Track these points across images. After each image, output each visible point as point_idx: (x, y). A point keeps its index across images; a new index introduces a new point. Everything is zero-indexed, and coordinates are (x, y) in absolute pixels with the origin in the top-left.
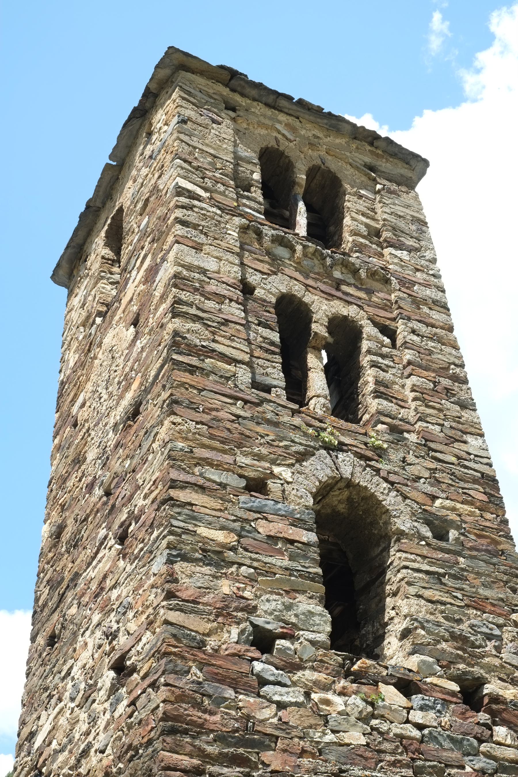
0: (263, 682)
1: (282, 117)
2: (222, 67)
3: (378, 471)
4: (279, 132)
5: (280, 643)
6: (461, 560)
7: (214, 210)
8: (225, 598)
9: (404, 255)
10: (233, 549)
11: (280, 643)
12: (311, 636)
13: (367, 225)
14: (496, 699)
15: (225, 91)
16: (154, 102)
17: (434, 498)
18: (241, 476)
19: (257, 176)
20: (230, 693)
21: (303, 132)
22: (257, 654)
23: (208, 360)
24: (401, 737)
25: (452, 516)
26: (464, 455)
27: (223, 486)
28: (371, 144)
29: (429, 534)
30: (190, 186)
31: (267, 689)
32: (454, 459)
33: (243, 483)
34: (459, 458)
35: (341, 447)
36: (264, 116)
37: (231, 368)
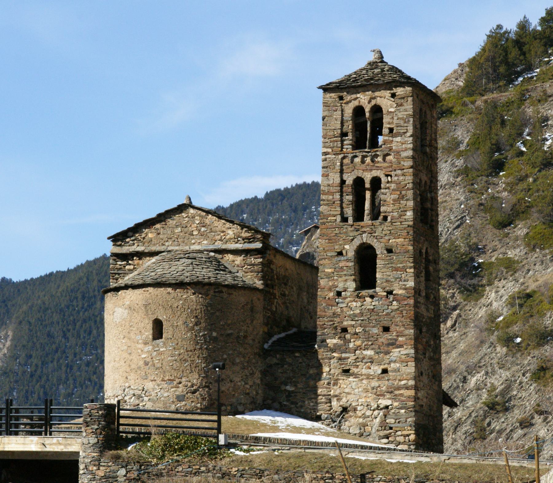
3: (374, 236)
5: (343, 293)
6: (394, 257)
8: (331, 286)
10: (333, 273)
17: (389, 240)
22: (337, 297)
23: (329, 218)
24: (368, 309)
25: (395, 244)
26: (403, 220)
27: (331, 256)
29: (386, 252)
32: (399, 223)
33: (336, 254)
34: (401, 222)
35: (365, 232)
37: (335, 218)
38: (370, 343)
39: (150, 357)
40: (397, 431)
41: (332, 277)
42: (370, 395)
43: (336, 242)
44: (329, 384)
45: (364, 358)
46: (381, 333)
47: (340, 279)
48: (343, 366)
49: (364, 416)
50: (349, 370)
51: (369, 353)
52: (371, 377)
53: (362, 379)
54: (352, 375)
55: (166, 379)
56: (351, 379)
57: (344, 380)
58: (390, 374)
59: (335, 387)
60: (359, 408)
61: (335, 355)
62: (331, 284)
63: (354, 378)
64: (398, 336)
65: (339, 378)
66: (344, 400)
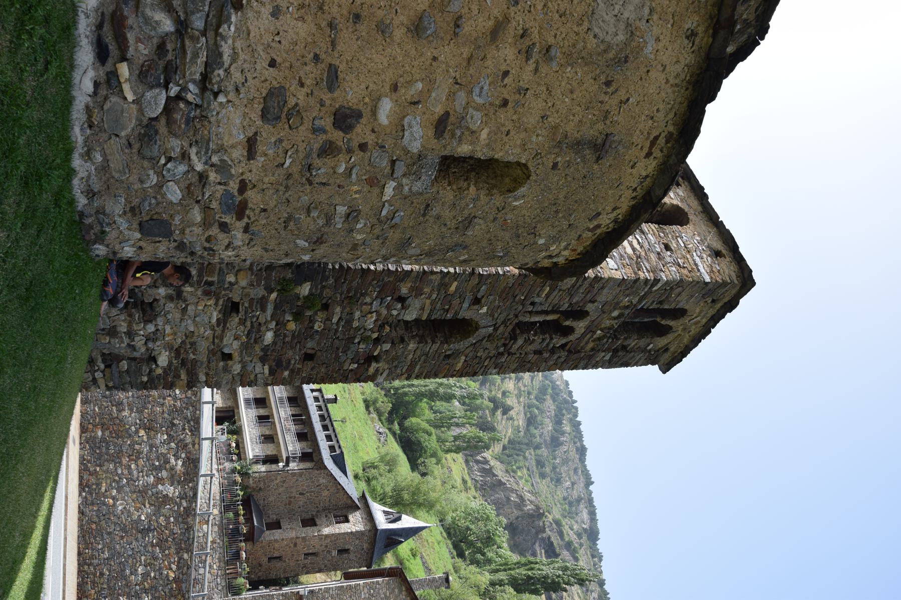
0: (382, 299)
1: (704, 320)
2: (738, 303)
4: (696, 317)
7: (643, 293)
9: (607, 358)
11: (399, 306)
12: (402, 314)
13: (629, 345)
14: (369, 366)
15: (726, 300)
16: (736, 260)
17: (466, 357)
18: (483, 297)
19: (666, 307)
20: (378, 289)
21: (694, 327)
28: (681, 352)
30: (659, 285)
31: (379, 300)
33: (479, 296)
35: (496, 329)
36: (707, 313)
38: (288, 339)
39: (370, 139)
40: (103, 372)
41: (439, 290)
42: (179, 341)
43: (500, 297)
44: (210, 284)
45: (259, 331)
46: (303, 352)
47: (428, 302)
48: (246, 305)
49: (130, 334)
50: (238, 312)
51: (269, 337)
52: (216, 341)
53: (213, 329)
54: (224, 316)
55: (250, 194)
56: (215, 316)
57: (216, 304)
58: (221, 364)
59: (199, 293)
60: (151, 328)
61: (274, 296)
62: (427, 290)
63: (218, 320)
64: (292, 371)
65: (221, 302)
66: (170, 306)
